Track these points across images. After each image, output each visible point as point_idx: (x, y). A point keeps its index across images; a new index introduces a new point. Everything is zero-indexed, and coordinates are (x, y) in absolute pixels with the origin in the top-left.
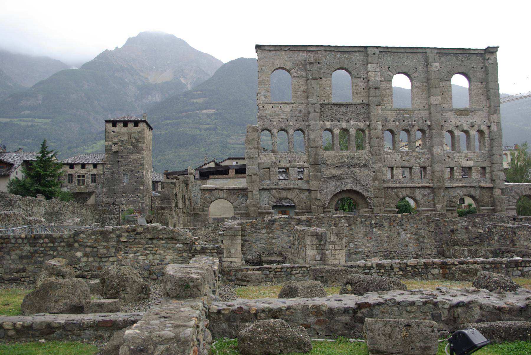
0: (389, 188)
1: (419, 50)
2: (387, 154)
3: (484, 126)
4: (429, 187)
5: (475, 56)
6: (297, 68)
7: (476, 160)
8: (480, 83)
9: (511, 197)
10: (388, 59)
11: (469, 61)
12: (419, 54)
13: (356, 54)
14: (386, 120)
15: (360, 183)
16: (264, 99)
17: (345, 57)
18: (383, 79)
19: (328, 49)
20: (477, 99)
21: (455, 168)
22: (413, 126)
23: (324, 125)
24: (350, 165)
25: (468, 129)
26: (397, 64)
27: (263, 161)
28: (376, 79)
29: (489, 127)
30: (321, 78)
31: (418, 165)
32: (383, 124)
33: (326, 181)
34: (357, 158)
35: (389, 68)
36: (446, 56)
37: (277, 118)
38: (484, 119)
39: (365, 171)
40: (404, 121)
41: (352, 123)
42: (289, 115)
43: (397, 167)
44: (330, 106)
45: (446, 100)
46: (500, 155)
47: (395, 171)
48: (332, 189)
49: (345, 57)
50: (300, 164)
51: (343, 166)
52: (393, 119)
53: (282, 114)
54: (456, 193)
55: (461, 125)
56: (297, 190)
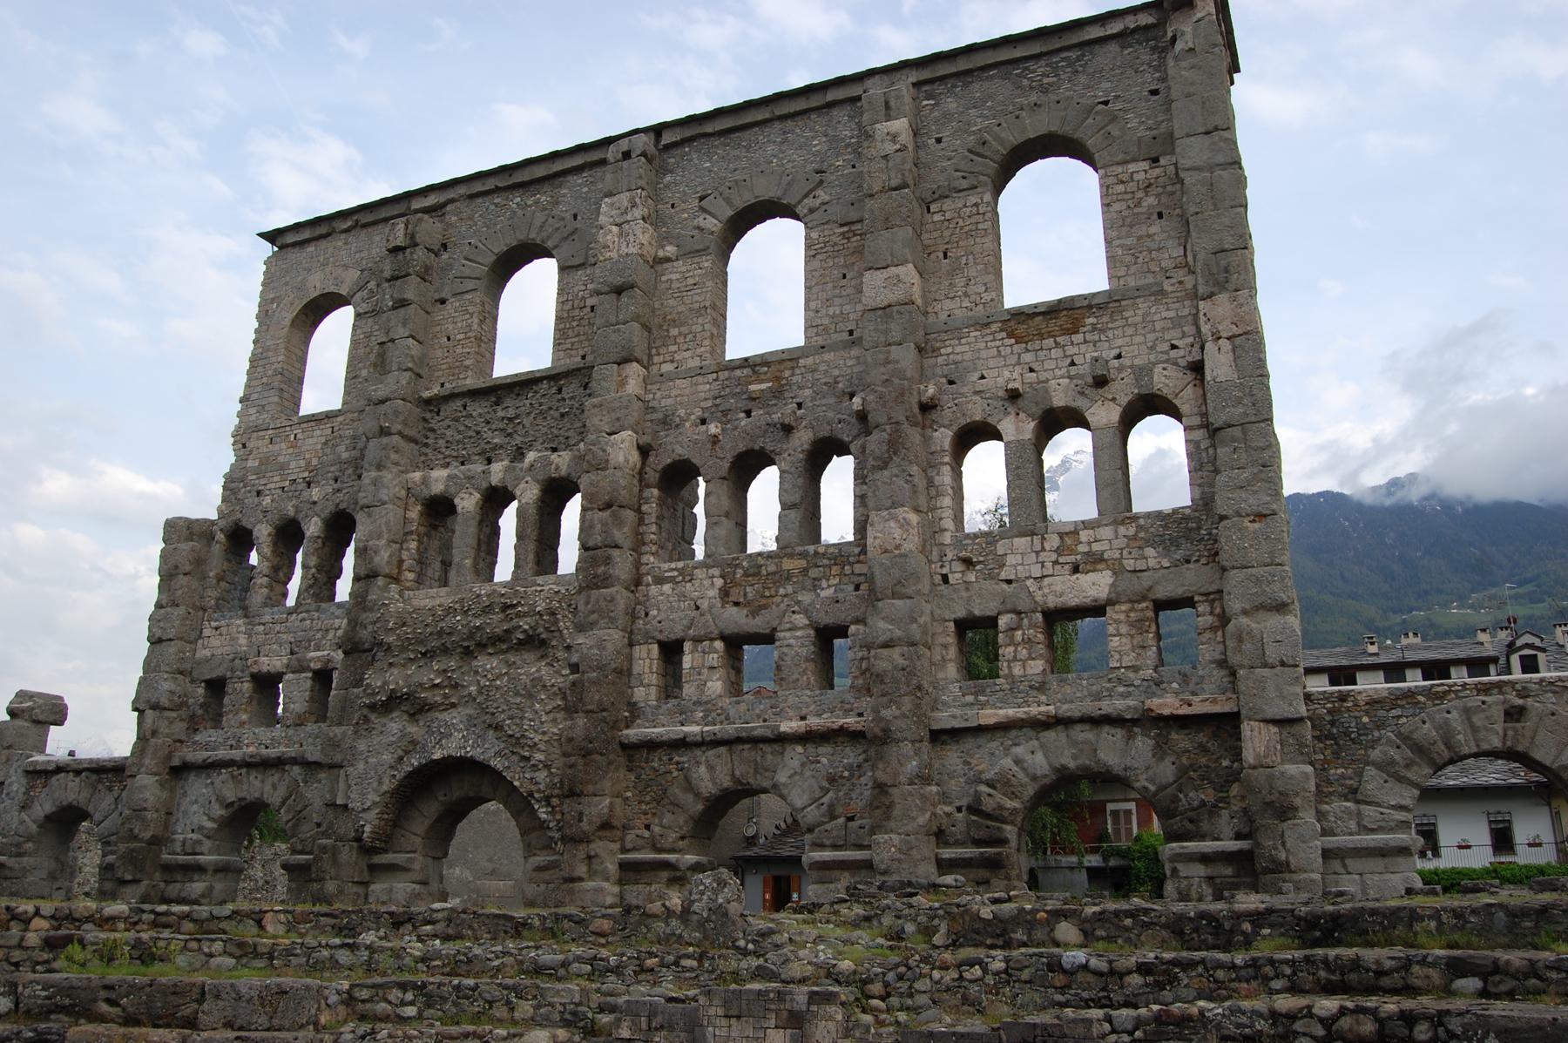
0: (651, 745)
1: (831, 96)
2: (660, 581)
3: (1172, 371)
4: (855, 736)
5: (1113, 47)
6: (372, 285)
7: (1129, 564)
8: (1145, 165)
9: (1370, 771)
10: (700, 166)
11: (1083, 79)
12: (835, 112)
13: (578, 180)
14: (666, 422)
15: (498, 727)
16: (253, 418)
17: (537, 202)
18: (670, 250)
19: (478, 187)
20: (1128, 242)
21: (1003, 621)
22: (787, 429)
23: (425, 481)
24: (471, 644)
25: (1080, 403)
26: (738, 176)
27: (207, 653)
28: (624, 250)
29: (1197, 368)
30: (443, 302)
31: (800, 620)
32: (646, 439)
33: (366, 720)
34: (505, 607)
35: (701, 199)
36: (966, 85)
37: (276, 481)
38: (1175, 333)
39: (531, 667)
40: (748, 413)
41: (531, 456)
42: (315, 462)
43: (697, 640)
44: (458, 403)
45: (959, 281)
46: (1260, 516)
47: (687, 661)
48: (387, 758)
49: (537, 202)
50: (315, 657)
51: (445, 650)
52: (698, 413)
53: (293, 465)
54: (1007, 762)
55: (1042, 388)
56: (296, 770)
